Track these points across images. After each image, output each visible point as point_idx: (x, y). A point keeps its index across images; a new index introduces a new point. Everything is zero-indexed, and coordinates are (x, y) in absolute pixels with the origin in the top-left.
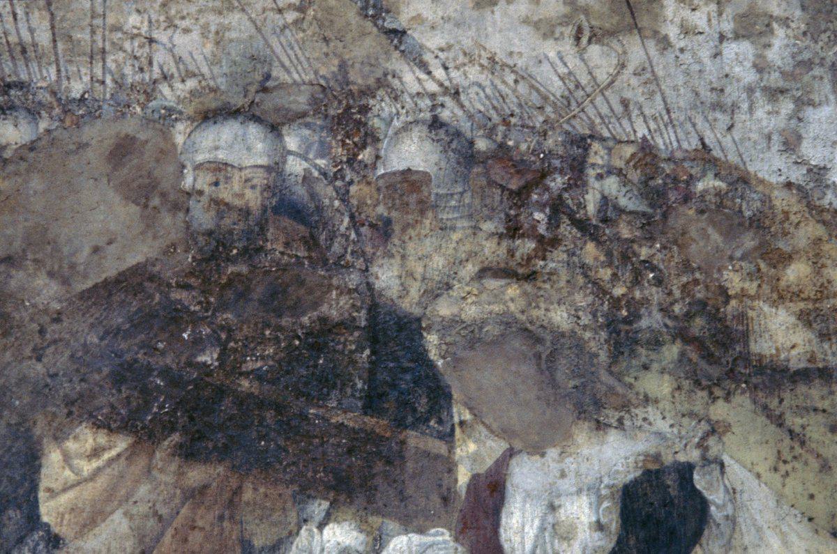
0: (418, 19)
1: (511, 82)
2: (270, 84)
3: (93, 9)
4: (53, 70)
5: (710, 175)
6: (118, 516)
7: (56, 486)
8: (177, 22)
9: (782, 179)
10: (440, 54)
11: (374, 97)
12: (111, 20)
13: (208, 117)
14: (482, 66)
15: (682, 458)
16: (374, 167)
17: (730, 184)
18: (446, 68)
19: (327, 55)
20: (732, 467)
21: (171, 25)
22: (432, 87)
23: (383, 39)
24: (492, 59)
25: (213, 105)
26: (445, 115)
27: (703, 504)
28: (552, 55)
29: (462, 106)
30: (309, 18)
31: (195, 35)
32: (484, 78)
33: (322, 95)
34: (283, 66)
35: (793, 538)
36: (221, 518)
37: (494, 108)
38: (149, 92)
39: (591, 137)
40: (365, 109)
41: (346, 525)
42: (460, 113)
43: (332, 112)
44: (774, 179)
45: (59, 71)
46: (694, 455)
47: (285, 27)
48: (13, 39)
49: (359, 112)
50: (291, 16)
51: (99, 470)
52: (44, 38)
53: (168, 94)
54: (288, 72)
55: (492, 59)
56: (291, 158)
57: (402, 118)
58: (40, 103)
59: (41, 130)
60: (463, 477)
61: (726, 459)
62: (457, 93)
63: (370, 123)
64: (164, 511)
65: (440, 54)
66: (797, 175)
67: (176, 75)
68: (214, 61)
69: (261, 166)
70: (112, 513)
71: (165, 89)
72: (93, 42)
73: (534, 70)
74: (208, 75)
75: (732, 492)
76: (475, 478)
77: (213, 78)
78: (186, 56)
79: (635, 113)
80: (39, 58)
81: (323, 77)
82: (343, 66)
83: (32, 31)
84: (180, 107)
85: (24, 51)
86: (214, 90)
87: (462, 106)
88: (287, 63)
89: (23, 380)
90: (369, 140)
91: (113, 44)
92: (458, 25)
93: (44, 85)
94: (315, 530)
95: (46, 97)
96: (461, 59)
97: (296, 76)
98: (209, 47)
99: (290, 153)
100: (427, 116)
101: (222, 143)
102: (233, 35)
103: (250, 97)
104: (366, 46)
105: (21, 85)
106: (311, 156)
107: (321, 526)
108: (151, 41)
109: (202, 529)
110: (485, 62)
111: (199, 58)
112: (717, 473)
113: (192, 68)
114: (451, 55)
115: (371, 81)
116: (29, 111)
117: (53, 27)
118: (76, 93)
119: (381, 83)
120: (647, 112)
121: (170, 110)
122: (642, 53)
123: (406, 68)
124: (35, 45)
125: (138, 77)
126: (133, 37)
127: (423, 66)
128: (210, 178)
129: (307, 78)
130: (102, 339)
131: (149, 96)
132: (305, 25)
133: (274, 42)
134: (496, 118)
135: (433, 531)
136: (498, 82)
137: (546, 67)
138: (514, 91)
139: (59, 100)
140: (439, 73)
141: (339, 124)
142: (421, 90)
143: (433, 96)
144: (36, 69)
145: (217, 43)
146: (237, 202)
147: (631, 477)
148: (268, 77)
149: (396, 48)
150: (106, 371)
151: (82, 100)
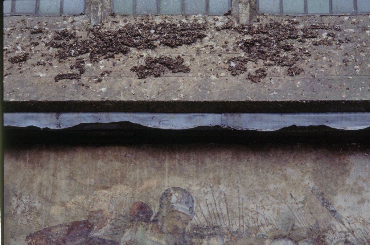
0: (340, 207)
2: (294, 228)
3: (239, 203)
4: (228, 222)
8: (265, 207)
10: (347, 219)
11: (327, 233)
12: (245, 206)
13: (275, 238)
14: (360, 223)
18: (349, 223)
19: (312, 218)
21: (263, 208)
22: (345, 230)
23: (330, 214)
24: (364, 221)
25: (277, 234)
26: (349, 239)
29: (355, 236)
30: (306, 206)
31: (271, 211)
32: (361, 227)
33: (311, 231)
34: (298, 222)
37: (365, 237)
38: (257, 230)
40: (324, 237)
42: (354, 238)
43: (314, 237)
45: (229, 222)
47: (299, 209)
48: (215, 212)
49: (322, 237)
50: (300, 205)
52: (225, 212)
53: (264, 230)
54: (300, 224)
55: (364, 221)
57: (336, 240)
58: (224, 233)
59: (225, 242)
62: (353, 232)
63: (326, 241)
65: (347, 219)
67: (265, 224)
68: (277, 220)
71: (262, 228)
72: (240, 213)
74: (275, 224)
77: (277, 226)
78: (269, 219)
80: (223, 218)
81: (311, 226)
82: (317, 222)
83: (221, 209)
84: (267, 235)
85: (219, 216)
86: (277, 229)
87: (355, 236)
88: (300, 221)
91: (246, 214)
92: (352, 209)
93: (225, 227)
95: (226, 231)
96: (354, 221)
97: (302, 225)
98: (275, 215)
100: (343, 239)
102: (282, 211)
103: (289, 232)
104: (324, 215)
105: (218, 227)
108: (257, 213)
110: (361, 222)
111: (272, 219)
113: (270, 222)
114: (351, 219)
115: (326, 228)
116: (221, 235)
117: (227, 208)
118: (235, 230)
119: (329, 228)
121: (264, 236)
123: (337, 223)
124: (222, 214)
125: (254, 225)
126: (252, 212)
127: (342, 222)
129: (306, 226)
131: (257, 231)
132: (305, 208)
133: (295, 213)
134: (365, 240)
136: (365, 228)
139: (230, 232)
140: (347, 225)
141: (316, 241)
142: (342, 231)
143: (345, 232)
144: (223, 222)
145: (278, 214)
148: (294, 225)
149: (334, 216)
151: (237, 232)
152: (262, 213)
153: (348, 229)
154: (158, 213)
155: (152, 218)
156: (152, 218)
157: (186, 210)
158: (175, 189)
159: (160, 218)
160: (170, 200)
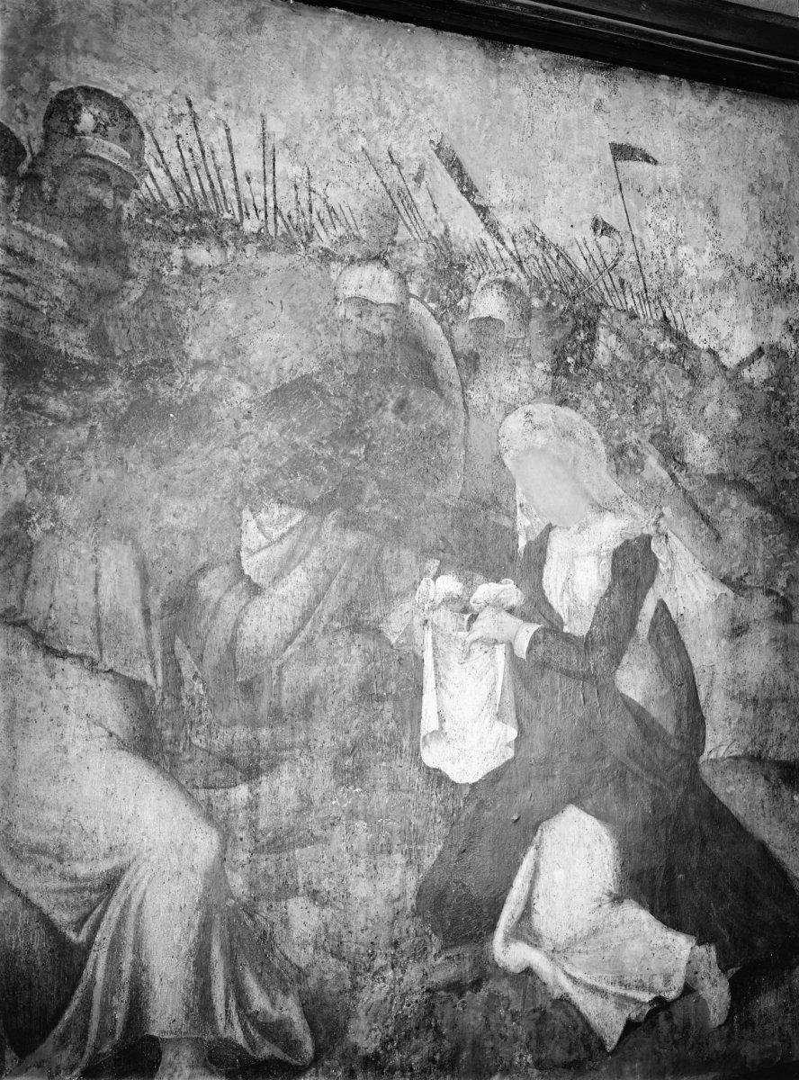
1: (555, 259)
5: (668, 339)
6: (299, 570)
7: (254, 547)
9: (706, 346)
15: (646, 532)
16: (468, 313)
17: (678, 347)
18: (514, 241)
20: (674, 540)
27: (656, 561)
28: (580, 240)
32: (538, 252)
34: (406, 225)
35: (700, 583)
36: (369, 572)
39: (602, 305)
41: (450, 577)
44: (701, 346)
46: (652, 530)
49: (458, 269)
51: (283, 536)
54: (410, 230)
56: (412, 300)
60: (522, 543)
61: (670, 534)
64: (329, 566)
66: (713, 344)
69: (391, 305)
70: (295, 567)
73: (569, 251)
75: (671, 554)
76: (529, 543)
77: (357, 229)
79: (627, 290)
88: (409, 224)
89: (225, 464)
90: (464, 292)
94: (432, 582)
99: (411, 295)
101: (363, 283)
106: (426, 300)
107: (435, 578)
109: (357, 580)
110: (538, 239)
112: (663, 541)
120: (635, 290)
122: (632, 245)
127: (500, 238)
128: (356, 311)
130: (282, 432)
135: (503, 581)
137: (576, 249)
138: (557, 265)
140: (510, 245)
146: (376, 332)
147: (618, 544)
150: (285, 459)
152: (321, 191)
153: (511, 254)
154: (42, 154)
155: (23, 168)
156: (23, 168)
157: (122, 158)
158: (90, 93)
159: (46, 171)
160: (77, 121)
